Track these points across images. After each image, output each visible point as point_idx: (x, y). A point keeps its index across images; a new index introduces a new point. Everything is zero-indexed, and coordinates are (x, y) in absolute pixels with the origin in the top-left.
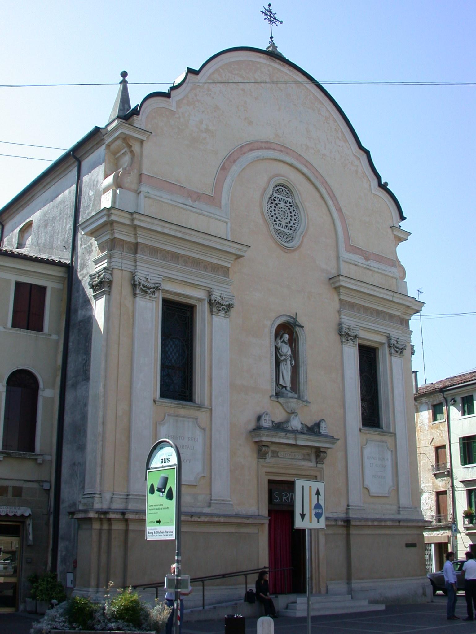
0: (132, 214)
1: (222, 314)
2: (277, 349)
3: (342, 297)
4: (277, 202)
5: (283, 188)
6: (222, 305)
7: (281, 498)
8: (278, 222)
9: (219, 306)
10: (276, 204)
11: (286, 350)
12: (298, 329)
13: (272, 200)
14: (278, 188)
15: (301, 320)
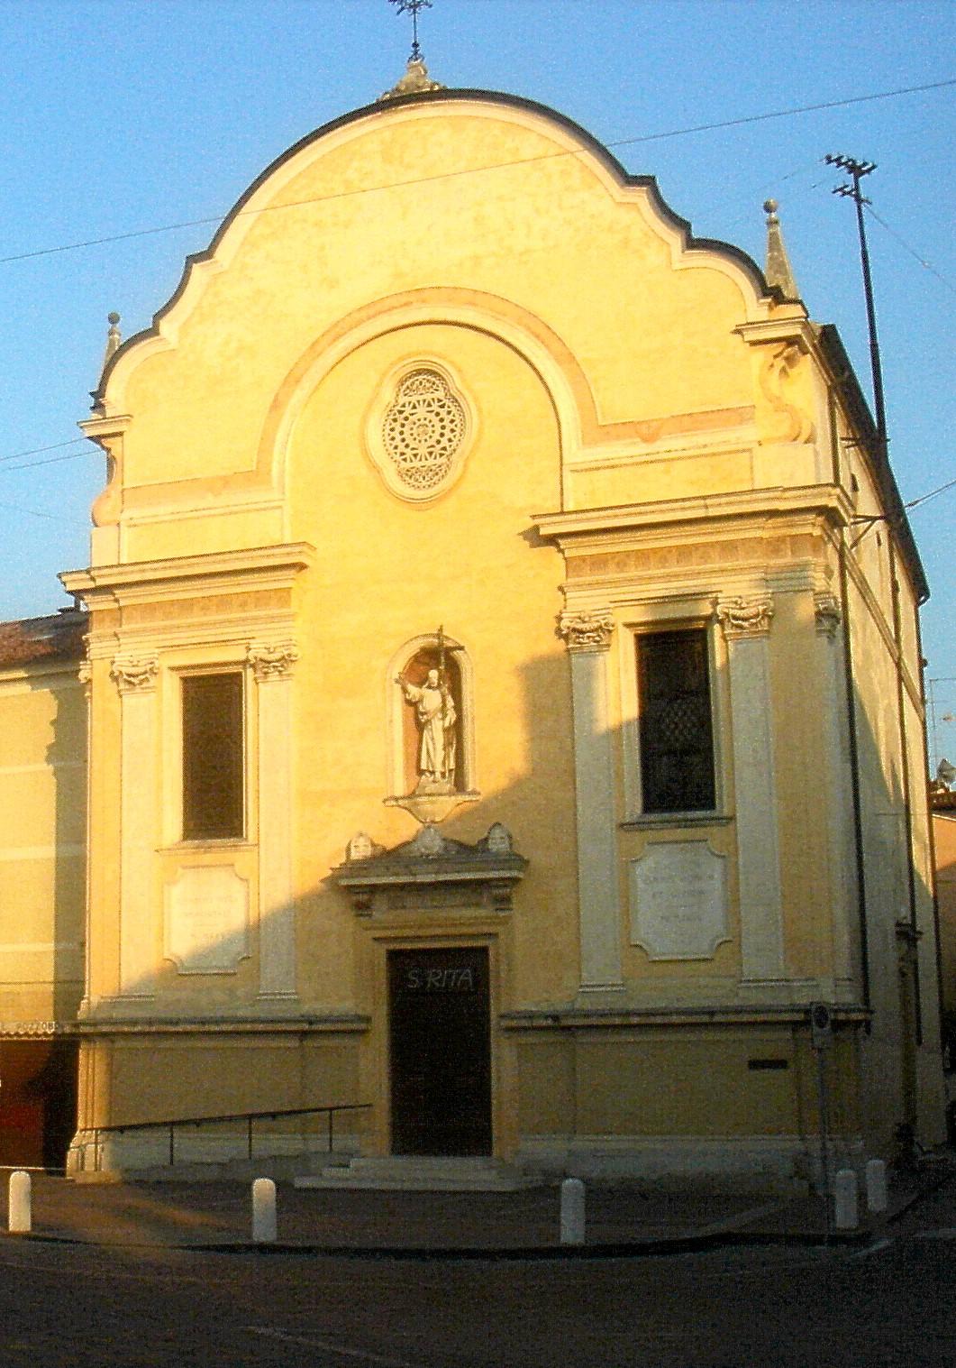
0: (88, 572)
1: (274, 676)
2: (412, 704)
3: (567, 554)
4: (408, 410)
5: (420, 378)
6: (269, 662)
7: (423, 977)
8: (409, 453)
9: (282, 664)
10: (406, 419)
11: (432, 699)
12: (457, 653)
13: (398, 416)
14: (408, 383)
15: (453, 636)
